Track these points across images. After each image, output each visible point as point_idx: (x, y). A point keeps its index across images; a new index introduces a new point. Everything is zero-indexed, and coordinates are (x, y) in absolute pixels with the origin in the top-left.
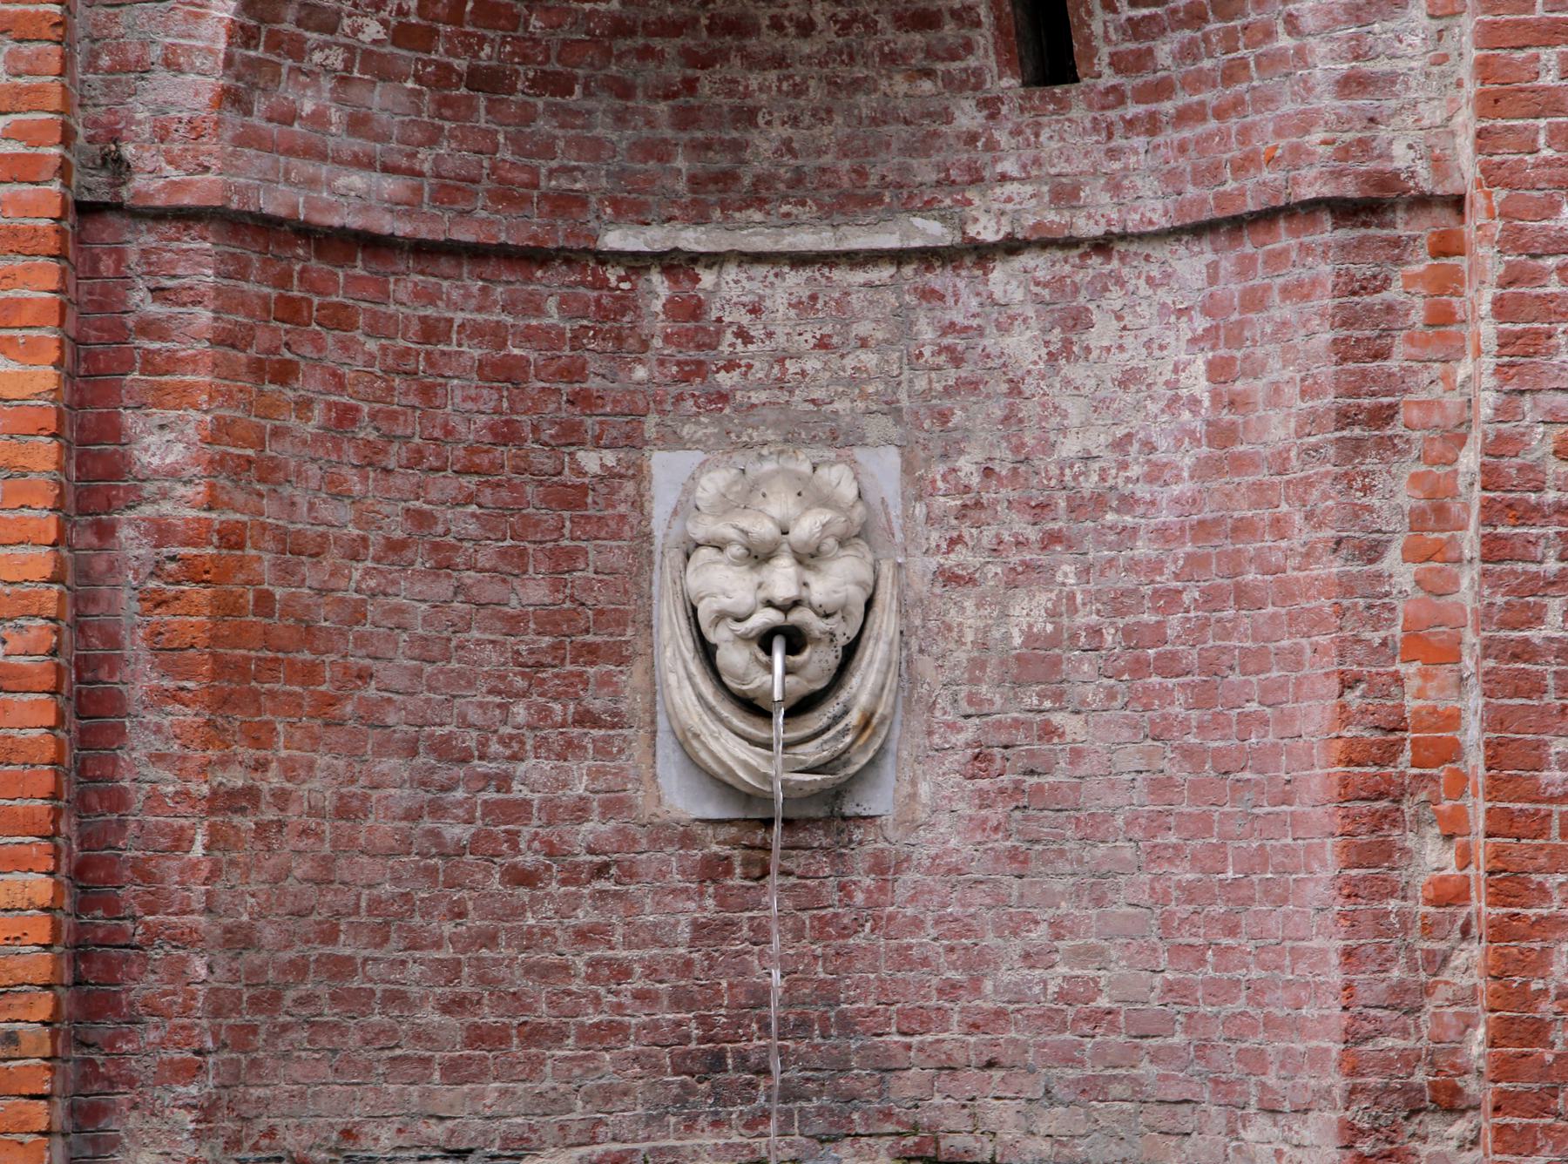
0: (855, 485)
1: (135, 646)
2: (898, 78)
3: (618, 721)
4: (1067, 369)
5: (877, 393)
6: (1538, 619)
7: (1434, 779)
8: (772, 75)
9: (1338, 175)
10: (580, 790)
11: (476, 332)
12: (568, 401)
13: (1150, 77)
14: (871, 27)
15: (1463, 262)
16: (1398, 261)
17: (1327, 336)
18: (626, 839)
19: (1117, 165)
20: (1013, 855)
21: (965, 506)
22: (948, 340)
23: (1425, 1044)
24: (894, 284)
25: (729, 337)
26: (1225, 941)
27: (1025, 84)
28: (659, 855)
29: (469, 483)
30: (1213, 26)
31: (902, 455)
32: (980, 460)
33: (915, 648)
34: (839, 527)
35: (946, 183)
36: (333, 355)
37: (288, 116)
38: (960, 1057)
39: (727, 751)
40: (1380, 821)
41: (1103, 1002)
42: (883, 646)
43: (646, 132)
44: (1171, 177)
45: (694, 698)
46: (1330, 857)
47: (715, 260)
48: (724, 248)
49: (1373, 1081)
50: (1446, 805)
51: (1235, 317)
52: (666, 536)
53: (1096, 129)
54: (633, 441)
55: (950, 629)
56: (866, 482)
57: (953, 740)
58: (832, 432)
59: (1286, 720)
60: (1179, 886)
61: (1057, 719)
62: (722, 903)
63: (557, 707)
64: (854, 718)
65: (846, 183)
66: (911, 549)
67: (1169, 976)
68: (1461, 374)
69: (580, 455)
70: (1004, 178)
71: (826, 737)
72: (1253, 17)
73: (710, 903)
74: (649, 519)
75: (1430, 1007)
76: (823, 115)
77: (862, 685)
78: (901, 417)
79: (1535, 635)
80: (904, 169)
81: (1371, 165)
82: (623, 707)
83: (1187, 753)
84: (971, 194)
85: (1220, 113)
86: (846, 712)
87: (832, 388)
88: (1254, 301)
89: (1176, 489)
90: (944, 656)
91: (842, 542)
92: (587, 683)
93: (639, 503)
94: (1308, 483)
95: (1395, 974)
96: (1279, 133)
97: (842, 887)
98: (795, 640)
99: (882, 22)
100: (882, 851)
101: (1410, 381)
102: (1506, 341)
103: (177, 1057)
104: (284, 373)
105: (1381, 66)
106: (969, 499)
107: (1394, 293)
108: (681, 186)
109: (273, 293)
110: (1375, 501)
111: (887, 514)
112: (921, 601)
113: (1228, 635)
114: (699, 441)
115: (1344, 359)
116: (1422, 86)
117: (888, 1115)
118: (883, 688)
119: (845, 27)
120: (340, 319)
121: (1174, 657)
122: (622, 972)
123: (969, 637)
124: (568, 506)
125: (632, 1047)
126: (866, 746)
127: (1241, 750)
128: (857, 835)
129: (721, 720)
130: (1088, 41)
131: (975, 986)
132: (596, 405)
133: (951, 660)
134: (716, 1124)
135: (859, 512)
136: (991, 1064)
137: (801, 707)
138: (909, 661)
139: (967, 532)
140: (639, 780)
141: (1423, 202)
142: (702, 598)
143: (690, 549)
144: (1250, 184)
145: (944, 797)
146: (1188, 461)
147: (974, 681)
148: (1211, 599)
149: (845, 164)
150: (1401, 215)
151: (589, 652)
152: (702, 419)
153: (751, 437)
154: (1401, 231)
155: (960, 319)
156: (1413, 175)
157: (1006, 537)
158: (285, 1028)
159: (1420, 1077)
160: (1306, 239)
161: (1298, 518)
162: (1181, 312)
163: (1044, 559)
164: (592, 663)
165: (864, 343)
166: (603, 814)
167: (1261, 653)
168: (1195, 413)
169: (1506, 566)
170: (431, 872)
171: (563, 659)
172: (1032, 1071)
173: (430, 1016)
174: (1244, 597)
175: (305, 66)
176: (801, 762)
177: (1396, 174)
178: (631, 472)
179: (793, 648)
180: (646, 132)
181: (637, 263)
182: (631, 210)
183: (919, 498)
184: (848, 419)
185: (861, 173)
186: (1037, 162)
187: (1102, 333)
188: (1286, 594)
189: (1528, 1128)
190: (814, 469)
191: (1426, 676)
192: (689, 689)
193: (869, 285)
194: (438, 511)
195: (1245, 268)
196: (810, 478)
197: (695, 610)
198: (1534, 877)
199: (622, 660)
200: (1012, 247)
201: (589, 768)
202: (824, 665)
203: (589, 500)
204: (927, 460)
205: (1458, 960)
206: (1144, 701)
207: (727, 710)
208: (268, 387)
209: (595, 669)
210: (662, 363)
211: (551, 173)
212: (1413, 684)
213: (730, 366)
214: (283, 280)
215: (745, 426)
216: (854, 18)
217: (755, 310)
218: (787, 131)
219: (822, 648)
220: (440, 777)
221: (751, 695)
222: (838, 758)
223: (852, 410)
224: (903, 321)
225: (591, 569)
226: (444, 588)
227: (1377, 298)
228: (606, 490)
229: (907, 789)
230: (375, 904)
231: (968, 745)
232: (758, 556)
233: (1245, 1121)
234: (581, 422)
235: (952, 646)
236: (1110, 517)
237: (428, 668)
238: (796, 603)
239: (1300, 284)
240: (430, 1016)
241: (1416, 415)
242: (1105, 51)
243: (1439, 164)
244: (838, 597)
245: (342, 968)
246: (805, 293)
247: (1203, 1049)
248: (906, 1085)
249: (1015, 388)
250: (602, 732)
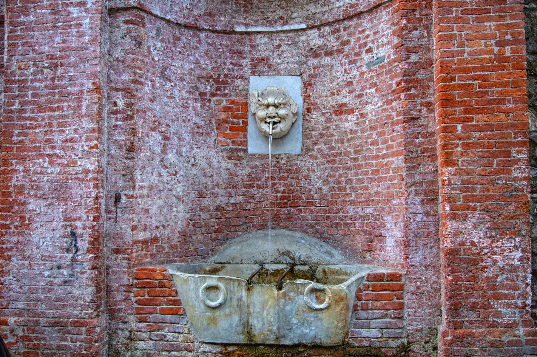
6: (13, 104)
169: (8, 94)
189: (6, 215)
198: (10, 161)
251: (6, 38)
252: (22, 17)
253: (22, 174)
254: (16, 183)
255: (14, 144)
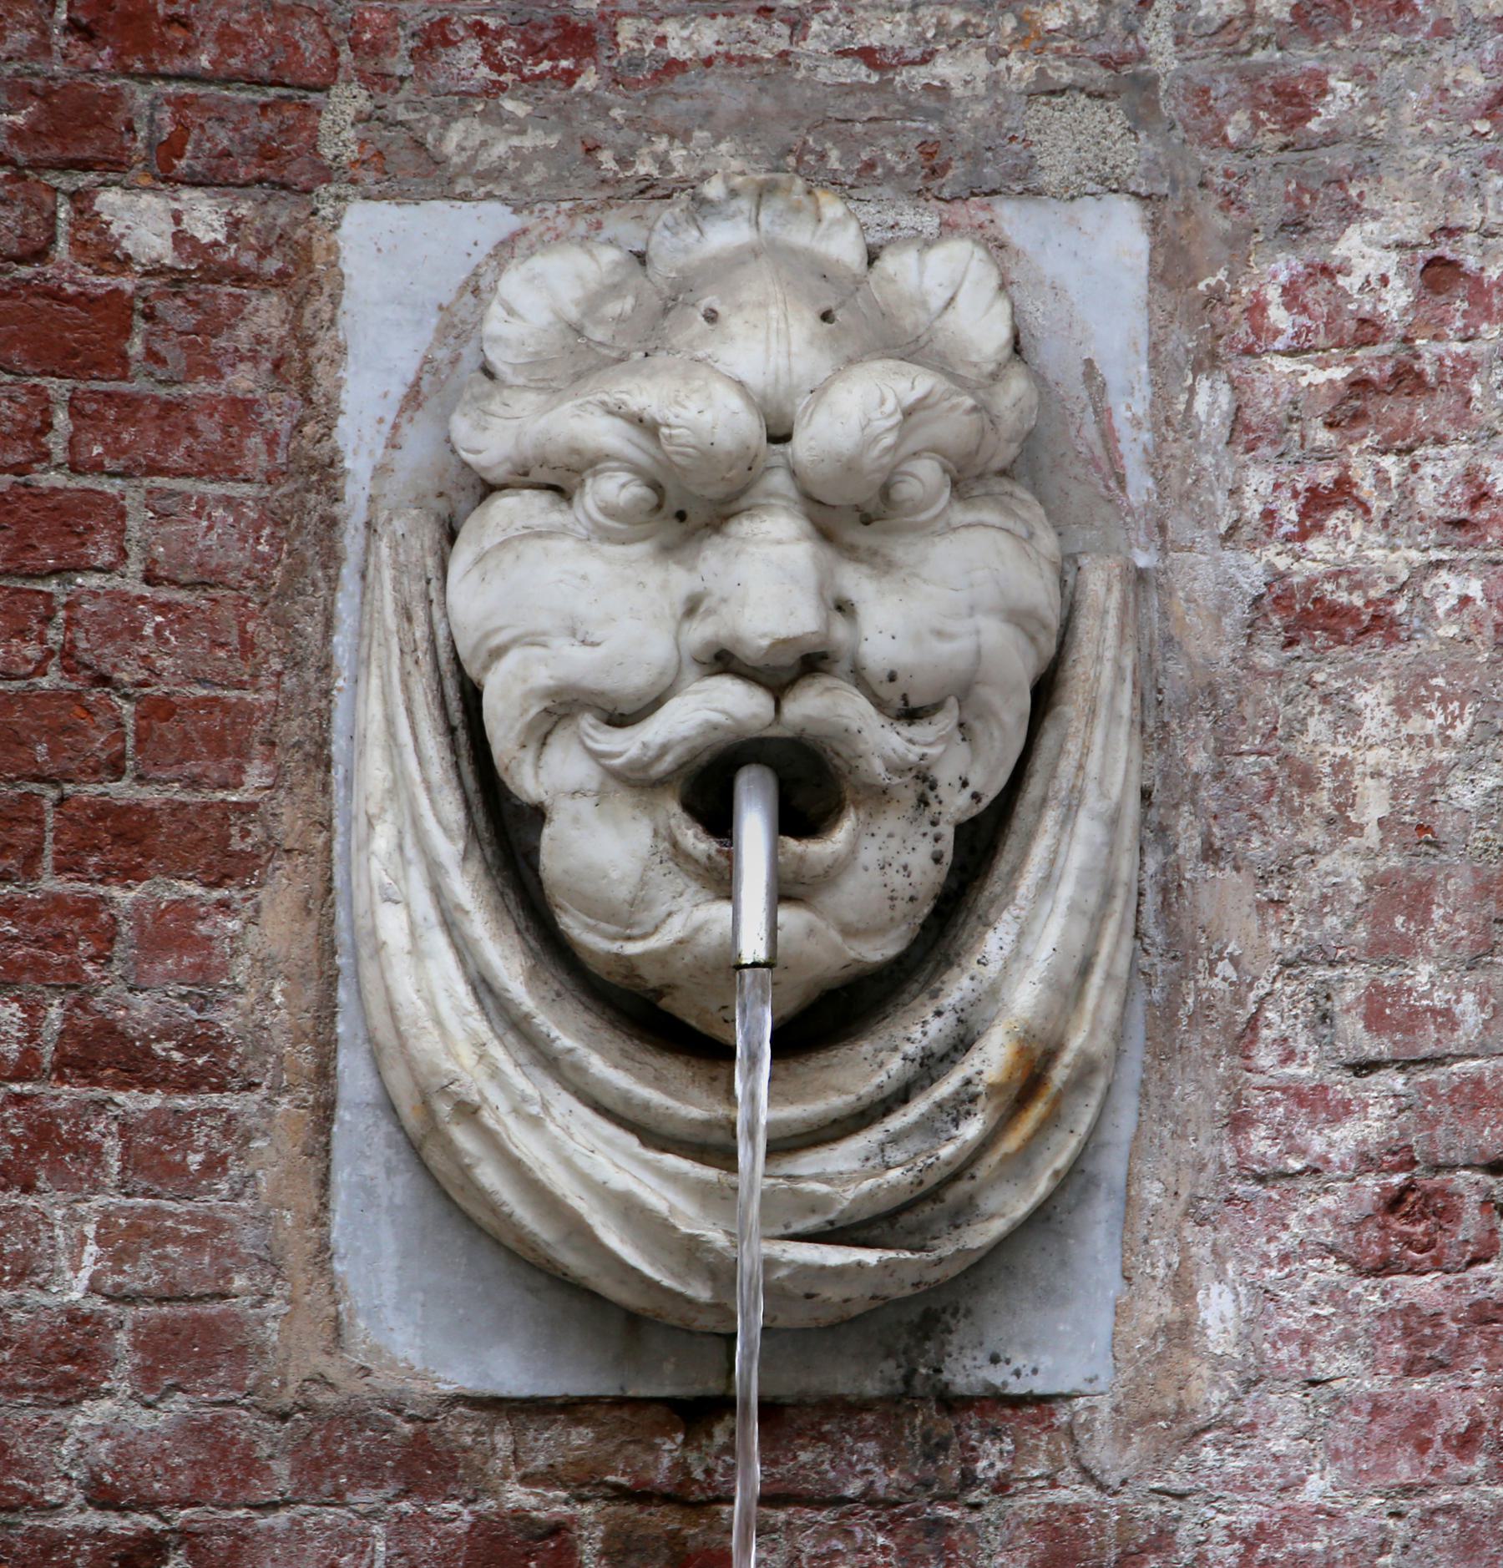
0: (1002, 308)
5: (1074, 29)
10: (75, 1291)
12: (73, 26)
21: (1360, 385)
28: (329, 1516)
31: (1154, 226)
32: (1412, 235)
33: (1189, 843)
39: (568, 1163)
42: (1087, 827)
45: (462, 989)
52: (381, 471)
55: (1306, 780)
56: (1038, 313)
57: (1318, 1145)
58: (928, 150)
66: (1180, 526)
69: (110, 201)
71: (896, 1122)
74: (328, 420)
77: (1017, 955)
78: (1153, 104)
82: (227, 1020)
86: (963, 1043)
87: (928, 15)
90: (1285, 869)
92: (107, 937)
100: (1075, 1513)
106: (1373, 361)
111: (1103, 415)
112: (1212, 690)
114: (495, 174)
118: (1085, 969)
123: (1373, 804)
126: (1026, 1156)
128: (991, 1460)
129: (549, 1061)
132: (166, 47)
133: (1313, 881)
138: (1171, 888)
140: (272, 1263)
142: (498, 653)
145: (1286, 1336)
151: (118, 837)
152: (509, 105)
153: (664, 163)
164: (130, 874)
166: (147, 1376)
171: (35, 854)
176: (815, 1204)
178: (272, 265)
183: (1208, 361)
184: (979, 110)
190: (872, 257)
192: (448, 958)
196: (858, 283)
197: (472, 695)
201: (106, 1219)
202: (898, 880)
203: (136, 347)
204: (1238, 244)
209: (138, 892)
215: (645, 128)
219: (891, 822)
221: (652, 977)
222: (933, 1195)
223: (994, 83)
225: (135, 567)
228: (191, 319)
229: (1159, 1308)
231: (1367, 1162)
234: (116, 95)
235: (1315, 835)
244: (952, 652)
250: (155, 1100)
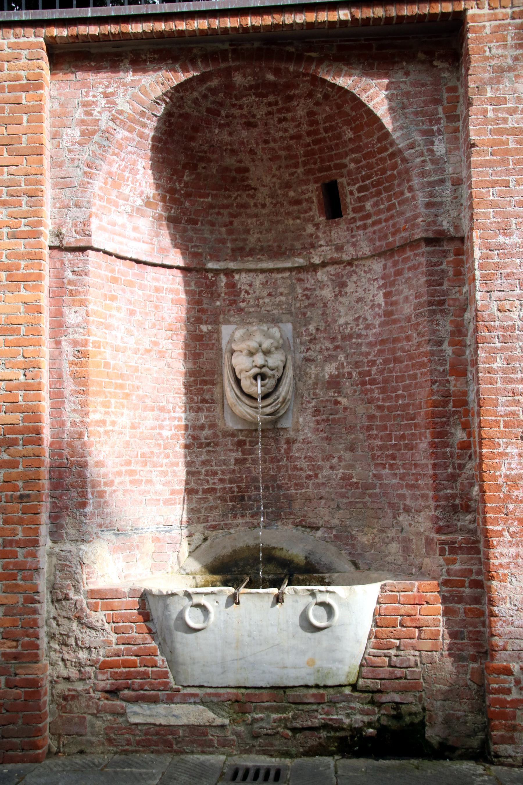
1: (67, 378)
2: (290, 219)
3: (213, 402)
4: (340, 299)
7: (460, 412)
8: (254, 220)
9: (427, 230)
10: (202, 421)
11: (171, 291)
13: (364, 213)
14: (282, 205)
15: (464, 257)
16: (445, 257)
17: (424, 279)
18: (215, 435)
19: (354, 240)
20: (327, 438)
22: (306, 292)
23: (459, 492)
24: (290, 277)
25: (243, 293)
26: (392, 462)
27: (328, 219)
29: (169, 333)
30: (384, 195)
34: (276, 344)
35: (304, 248)
36: (128, 295)
37: (114, 224)
38: (312, 496)
40: (443, 424)
41: (354, 480)
43: (219, 236)
44: (371, 241)
46: (428, 436)
47: (239, 271)
48: (242, 267)
49: (443, 503)
50: (463, 419)
51: (392, 279)
53: (348, 229)
54: (216, 322)
59: (411, 396)
60: (377, 446)
61: (339, 399)
62: (243, 453)
63: (196, 398)
64: (281, 399)
65: (275, 250)
67: (374, 472)
68: (464, 290)
69: (201, 326)
70: (321, 246)
72: (397, 190)
73: (240, 453)
75: (460, 480)
76: (269, 231)
79: (495, 366)
80: (292, 245)
81: (437, 228)
83: (379, 408)
84: (311, 250)
85: (386, 220)
86: (278, 398)
88: (398, 273)
89: (374, 331)
91: (277, 348)
93: (218, 340)
94: (418, 324)
95: (449, 471)
96: (406, 222)
97: (277, 448)
98: (264, 377)
99: (285, 203)
101: (449, 292)
102: (483, 276)
103: (80, 500)
104: (113, 298)
105: (438, 199)
106: (312, 337)
107: (444, 266)
108: (229, 251)
109: (110, 275)
110: (440, 328)
113: (392, 372)
115: (430, 286)
116: (450, 206)
117: (291, 514)
119: (275, 205)
120: (130, 284)
121: (375, 379)
122: (215, 473)
123: (313, 376)
124: (198, 341)
125: (218, 495)
127: (396, 405)
129: (241, 401)
130: (345, 204)
131: (316, 476)
134: (243, 516)
135: (281, 341)
136: (321, 498)
137: (265, 397)
139: (312, 346)
141: (452, 239)
143: (232, 352)
144: (397, 238)
146: (378, 322)
147: (315, 389)
148: (386, 362)
149: (276, 244)
150: (445, 243)
154: (445, 248)
155: (308, 286)
156: (449, 231)
157: (323, 347)
158: (115, 491)
159: (457, 502)
160: (416, 252)
161: (415, 335)
162: (374, 280)
163: (334, 353)
165: (281, 294)
167: (403, 376)
168: (380, 308)
170: (159, 445)
172: (333, 500)
173: (159, 487)
174: (397, 360)
175: (119, 210)
177: (444, 230)
179: (263, 379)
180: (219, 236)
181: (216, 272)
182: (216, 257)
183: (298, 337)
185: (280, 247)
186: (331, 241)
187: (350, 288)
188: (411, 358)
191: (456, 380)
193: (283, 278)
194: (160, 341)
195: (395, 264)
198: (497, 440)
199: (214, 384)
200: (324, 265)
204: (300, 327)
205: (468, 466)
206: (366, 392)
207: (244, 398)
208: (108, 302)
210: (224, 300)
211: (192, 247)
212: (453, 383)
213: (244, 301)
214: (113, 271)
216: (277, 203)
217: (250, 285)
218: (259, 236)
220: (162, 417)
224: (292, 288)
226: (162, 363)
227: (439, 268)
229: (296, 420)
230: (143, 455)
232: (251, 354)
233: (399, 514)
236: (354, 340)
237: (157, 386)
238: (264, 366)
239: (414, 265)
240: (159, 487)
241: (451, 302)
242: (350, 207)
243: (457, 228)
244: (276, 365)
245: (132, 473)
246: (264, 281)
247: (385, 494)
248: (297, 505)
249: (325, 305)
251: (476, 266)
252: (500, 237)
253: (516, 458)
254: (508, 472)
255: (501, 416)
